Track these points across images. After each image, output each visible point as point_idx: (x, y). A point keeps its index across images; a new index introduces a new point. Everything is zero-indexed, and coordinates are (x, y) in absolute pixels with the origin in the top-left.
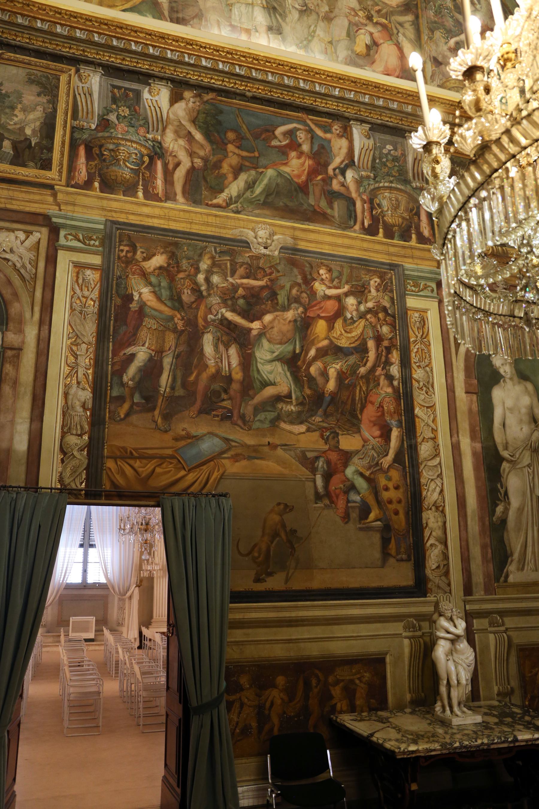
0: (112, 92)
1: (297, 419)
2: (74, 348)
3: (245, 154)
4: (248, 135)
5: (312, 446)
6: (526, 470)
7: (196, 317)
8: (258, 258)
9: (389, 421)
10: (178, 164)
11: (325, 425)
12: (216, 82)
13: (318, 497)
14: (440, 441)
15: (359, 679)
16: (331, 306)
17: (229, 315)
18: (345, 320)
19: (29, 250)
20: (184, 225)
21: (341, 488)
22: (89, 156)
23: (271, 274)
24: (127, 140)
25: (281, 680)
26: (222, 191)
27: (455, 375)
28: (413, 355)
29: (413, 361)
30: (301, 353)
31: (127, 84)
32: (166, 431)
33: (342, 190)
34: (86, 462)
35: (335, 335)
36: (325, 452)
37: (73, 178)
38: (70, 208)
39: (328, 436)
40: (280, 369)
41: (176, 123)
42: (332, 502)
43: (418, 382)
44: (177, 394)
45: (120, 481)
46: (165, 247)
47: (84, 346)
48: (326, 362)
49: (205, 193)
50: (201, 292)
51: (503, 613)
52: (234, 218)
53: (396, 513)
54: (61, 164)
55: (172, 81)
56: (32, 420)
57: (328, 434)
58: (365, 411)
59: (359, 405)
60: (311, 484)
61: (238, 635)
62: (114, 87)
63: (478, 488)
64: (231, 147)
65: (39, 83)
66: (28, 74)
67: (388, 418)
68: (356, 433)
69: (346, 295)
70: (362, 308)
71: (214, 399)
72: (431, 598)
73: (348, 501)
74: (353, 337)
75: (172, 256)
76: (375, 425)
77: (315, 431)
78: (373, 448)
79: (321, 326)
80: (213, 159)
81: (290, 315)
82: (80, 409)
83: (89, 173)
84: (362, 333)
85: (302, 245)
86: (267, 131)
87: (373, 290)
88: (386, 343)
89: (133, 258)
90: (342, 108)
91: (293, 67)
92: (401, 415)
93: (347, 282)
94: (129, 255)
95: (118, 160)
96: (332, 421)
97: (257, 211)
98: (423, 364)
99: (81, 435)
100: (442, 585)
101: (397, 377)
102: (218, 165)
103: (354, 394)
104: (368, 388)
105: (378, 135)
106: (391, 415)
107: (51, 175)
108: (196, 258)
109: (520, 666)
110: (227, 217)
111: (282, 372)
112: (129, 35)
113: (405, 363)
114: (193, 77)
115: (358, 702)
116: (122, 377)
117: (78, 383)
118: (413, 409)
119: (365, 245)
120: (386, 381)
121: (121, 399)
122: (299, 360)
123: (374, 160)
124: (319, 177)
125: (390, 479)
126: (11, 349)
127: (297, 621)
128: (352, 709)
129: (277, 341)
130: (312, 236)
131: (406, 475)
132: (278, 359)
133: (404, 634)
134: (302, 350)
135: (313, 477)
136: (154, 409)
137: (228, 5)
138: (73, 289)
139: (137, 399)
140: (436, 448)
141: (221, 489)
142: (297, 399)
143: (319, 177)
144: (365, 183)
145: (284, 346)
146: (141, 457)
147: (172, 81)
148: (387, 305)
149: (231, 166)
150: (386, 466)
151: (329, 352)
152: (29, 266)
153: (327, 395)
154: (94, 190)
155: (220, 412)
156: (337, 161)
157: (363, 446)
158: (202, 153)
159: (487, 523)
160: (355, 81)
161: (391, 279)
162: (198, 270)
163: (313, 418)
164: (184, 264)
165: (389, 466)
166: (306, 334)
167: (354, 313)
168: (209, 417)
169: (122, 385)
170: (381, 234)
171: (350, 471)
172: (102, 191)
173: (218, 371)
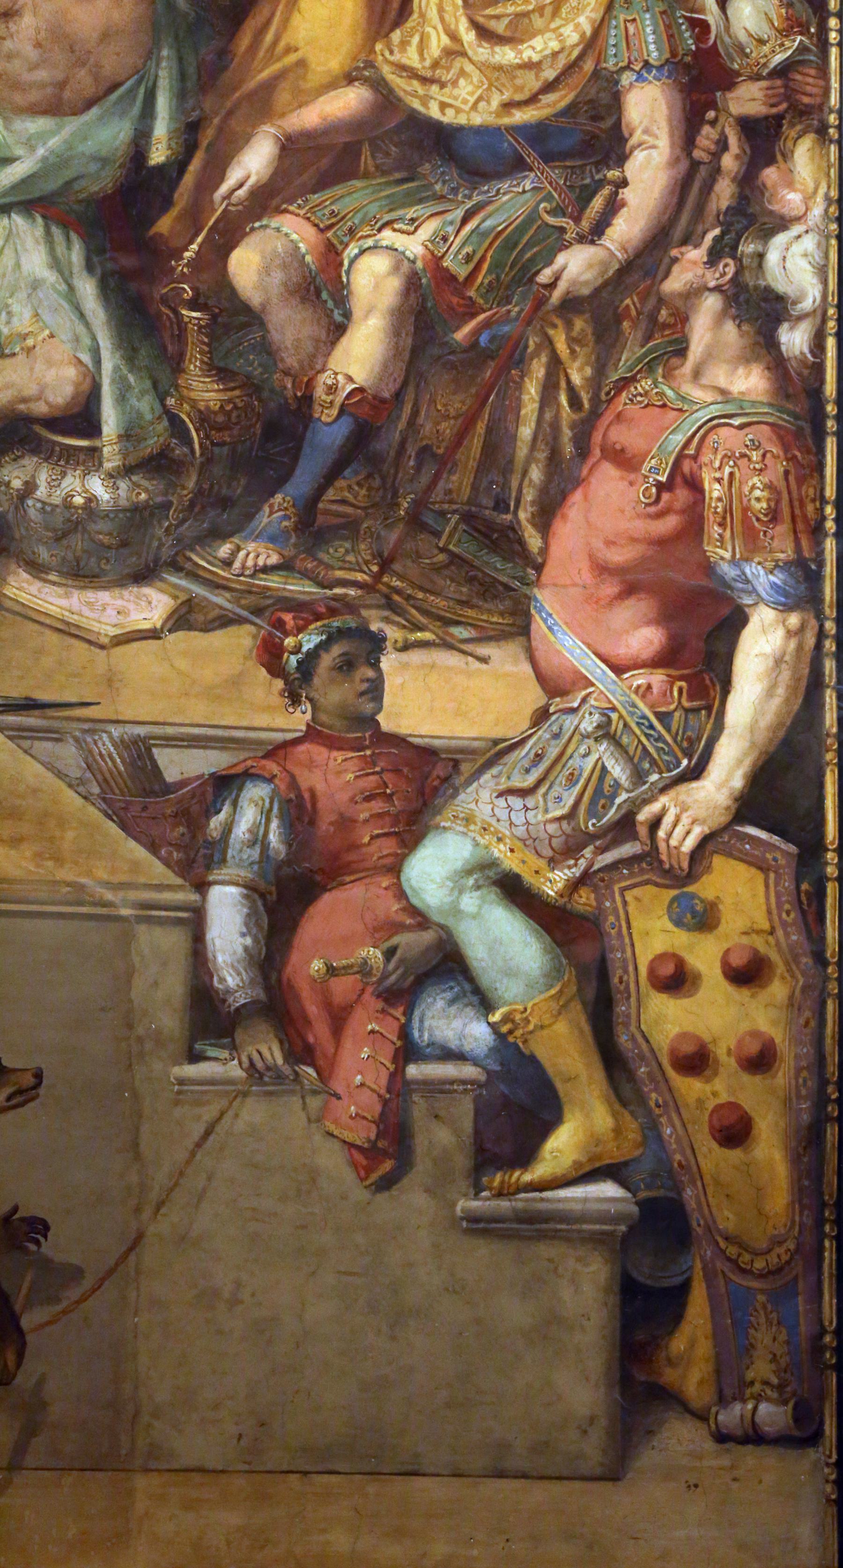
9: (728, 571)
21: (364, 969)
30: (180, 164)
35: (411, 58)
39: (313, 655)
48: (338, 219)
57: (310, 641)
59: (536, 474)
68: (499, 636)
74: (529, 66)
76: (629, 590)
77: (225, 621)
92: (817, 531)
101: (807, 304)
104: (600, 370)
111: (50, 277)
120: (730, 329)
122: (167, 203)
129: (34, 96)
131: (820, 894)
134: (190, 149)
135: (193, 897)
142: (128, 436)
145: (72, 125)
151: (366, 159)
153: (329, 415)
157: (541, 716)
163: (224, 550)
165: (705, 841)
166: (224, 54)
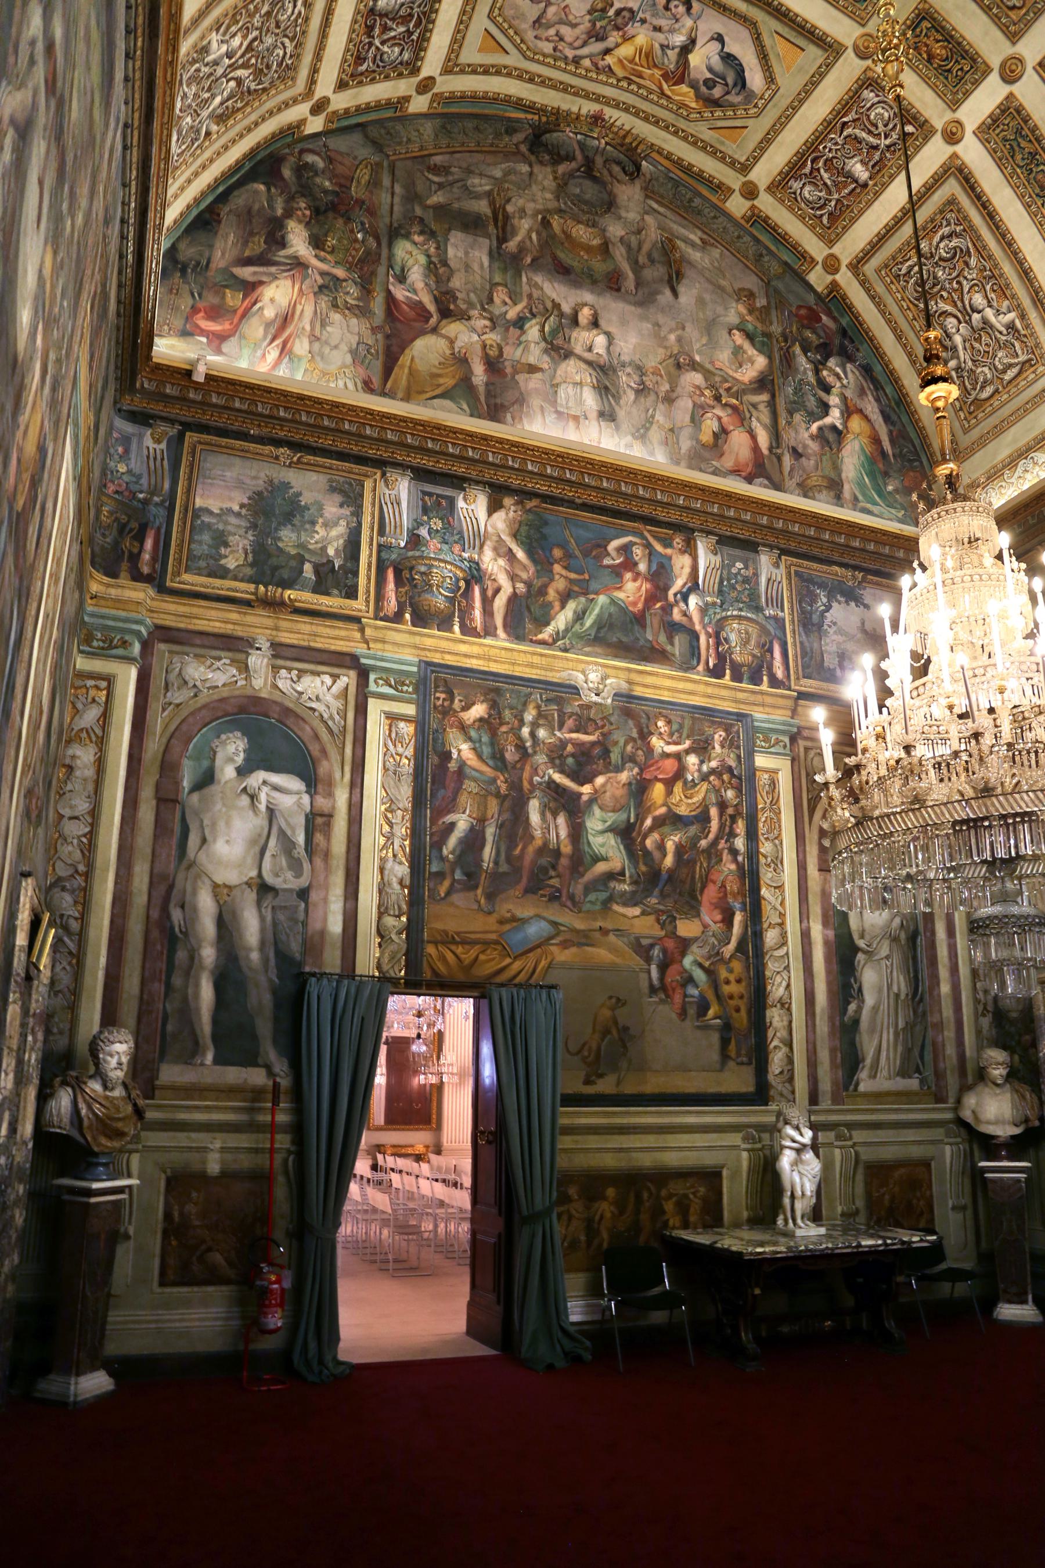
0: (423, 500)
1: (630, 900)
2: (389, 815)
3: (573, 576)
4: (577, 553)
5: (646, 932)
6: (883, 962)
7: (521, 779)
8: (588, 707)
10: (497, 590)
11: (661, 907)
12: (543, 488)
13: (653, 990)
14: (789, 928)
15: (694, 1193)
16: (670, 765)
17: (558, 777)
18: (685, 782)
19: (336, 697)
20: (506, 666)
22: (399, 582)
23: (603, 727)
24: (440, 560)
25: (611, 1192)
26: (548, 624)
27: (808, 849)
28: (761, 825)
29: (760, 832)
31: (439, 490)
32: (490, 913)
34: (405, 946)
36: (661, 939)
37: (382, 609)
38: (379, 646)
40: (613, 842)
41: (495, 538)
43: (766, 857)
44: (501, 870)
45: (442, 968)
46: (485, 695)
47: (399, 813)
49: (529, 626)
50: (525, 749)
51: (851, 1126)
52: (562, 658)
53: (738, 1010)
54: (368, 591)
55: (491, 485)
56: (346, 899)
58: (706, 891)
61: (565, 1142)
62: (425, 493)
63: (829, 983)
64: (557, 568)
65: (341, 491)
66: (330, 481)
69: (687, 752)
70: (705, 768)
71: (541, 877)
72: (773, 1107)
73: (685, 996)
75: (494, 705)
78: (714, 935)
79: (658, 790)
80: (538, 583)
81: (624, 776)
82: (396, 886)
83: (399, 602)
84: (704, 799)
85: (639, 691)
86: (599, 546)
87: (717, 747)
88: (730, 811)
89: (450, 708)
93: (688, 737)
94: (446, 704)
95: (431, 586)
96: (670, 903)
97: (587, 649)
98: (771, 836)
99: (399, 916)
100: (785, 1092)
102: (542, 591)
103: (694, 872)
105: (727, 550)
106: (734, 896)
107: (357, 605)
108: (520, 707)
109: (867, 1184)
110: (554, 657)
112: (447, 436)
113: (752, 835)
114: (515, 482)
115: (692, 1219)
116: (441, 850)
117: (395, 856)
118: (759, 889)
119: (710, 690)
121: (440, 875)
124: (658, 605)
125: (731, 971)
126: (322, 815)
127: (629, 1128)
128: (686, 1225)
130: (649, 680)
132: (611, 829)
133: (744, 1146)
136: (476, 887)
137: (553, 386)
138: (385, 745)
139: (458, 875)
140: (784, 935)
141: (549, 981)
142: (631, 877)
143: (658, 605)
144: (711, 611)
146: (464, 942)
147: (491, 485)
148: (733, 763)
149: (558, 592)
152: (337, 717)
154: (405, 623)
155: (547, 891)
156: (679, 584)
158: (524, 576)
159: (837, 1023)
160: (703, 489)
161: (738, 732)
162: (522, 722)
164: (507, 714)
167: (696, 775)
168: (535, 897)
169: (442, 859)
170: (728, 677)
171: (687, 961)
172: (414, 625)
173: (546, 844)
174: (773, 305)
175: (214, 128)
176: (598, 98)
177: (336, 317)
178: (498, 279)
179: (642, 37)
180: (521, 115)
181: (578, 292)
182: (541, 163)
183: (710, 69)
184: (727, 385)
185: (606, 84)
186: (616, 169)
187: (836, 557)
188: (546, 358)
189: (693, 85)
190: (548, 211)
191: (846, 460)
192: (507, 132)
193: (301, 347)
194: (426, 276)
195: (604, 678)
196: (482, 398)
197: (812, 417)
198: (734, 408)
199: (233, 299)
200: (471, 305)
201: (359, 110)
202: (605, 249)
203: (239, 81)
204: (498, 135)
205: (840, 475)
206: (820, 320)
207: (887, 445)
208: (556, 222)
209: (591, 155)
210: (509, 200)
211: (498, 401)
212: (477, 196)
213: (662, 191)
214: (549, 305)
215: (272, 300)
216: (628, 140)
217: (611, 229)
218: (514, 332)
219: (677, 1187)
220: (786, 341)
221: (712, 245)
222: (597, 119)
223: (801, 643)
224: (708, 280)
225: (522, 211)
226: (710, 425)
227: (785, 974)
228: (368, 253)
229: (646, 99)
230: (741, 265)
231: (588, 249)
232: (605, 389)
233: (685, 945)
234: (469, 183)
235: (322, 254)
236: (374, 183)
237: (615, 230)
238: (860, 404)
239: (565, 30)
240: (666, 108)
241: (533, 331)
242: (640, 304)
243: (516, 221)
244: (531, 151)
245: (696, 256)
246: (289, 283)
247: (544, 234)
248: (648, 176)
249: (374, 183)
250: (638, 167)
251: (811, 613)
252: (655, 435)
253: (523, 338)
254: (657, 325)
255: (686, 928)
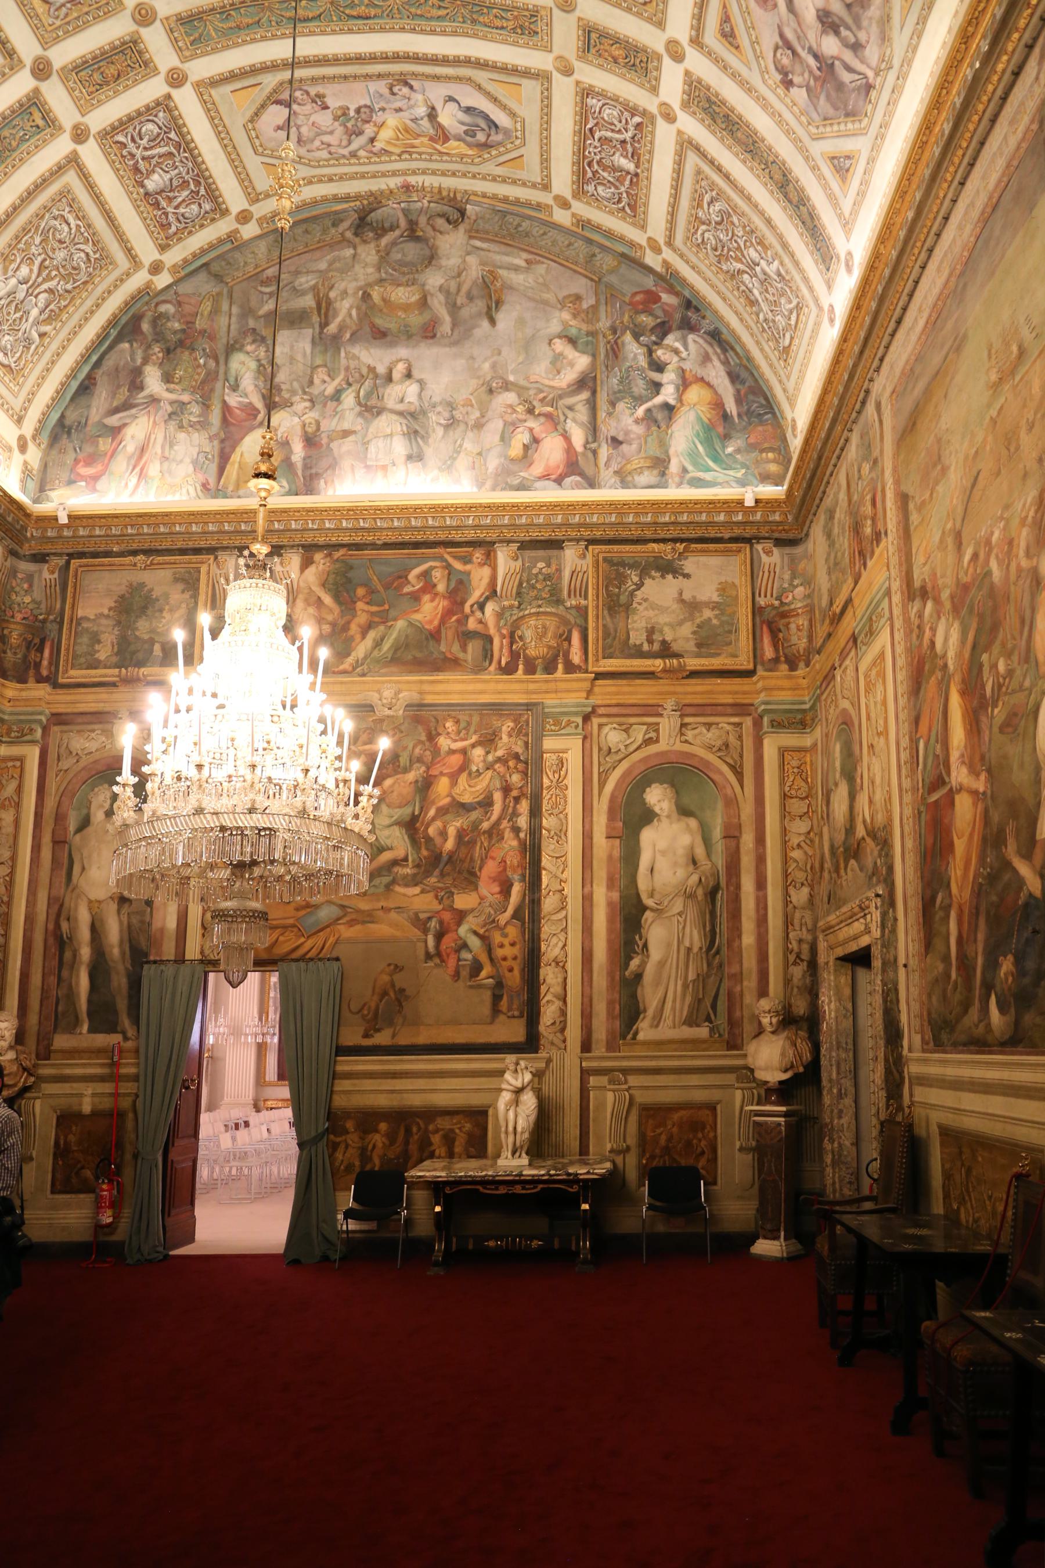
1: (413, 881)
3: (374, 609)
4: (380, 587)
5: (425, 907)
13: (428, 956)
16: (456, 760)
18: (470, 774)
26: (349, 655)
27: (595, 819)
28: (545, 802)
33: (479, 628)
36: (438, 912)
40: (398, 833)
42: (442, 961)
43: (549, 831)
51: (626, 1071)
53: (511, 970)
55: (303, 546)
60: (422, 945)
63: (610, 942)
64: (360, 605)
67: (509, 874)
69: (473, 746)
70: (490, 758)
72: (543, 1054)
73: (459, 960)
79: (443, 785)
80: (341, 622)
81: (411, 776)
85: (429, 699)
86: (400, 577)
90: (482, 535)
91: (417, 509)
93: (475, 732)
96: (449, 881)
97: (383, 671)
98: (556, 811)
110: (353, 682)
114: (321, 540)
115: (458, 1149)
118: (539, 861)
119: (500, 687)
123: (520, 584)
124: (454, 618)
125: (506, 936)
132: (398, 823)
144: (507, 614)
148: (519, 749)
149: (359, 626)
150: (502, 922)
156: (476, 596)
158: (330, 618)
159: (617, 978)
167: (481, 765)
171: (463, 930)
174: (603, 301)
175: (46, 328)
176: (394, 174)
177: (182, 436)
178: (318, 361)
179: (392, 121)
180: (345, 206)
181: (394, 351)
182: (365, 242)
183: (463, 123)
184: (541, 396)
185: (391, 161)
186: (440, 222)
187: (648, 534)
188: (360, 420)
189: (458, 138)
190: (370, 285)
191: (676, 434)
192: (334, 225)
193: (154, 469)
194: (256, 379)
195: (398, 693)
196: (300, 473)
197: (639, 400)
198: (548, 416)
199: (104, 444)
200: (294, 393)
201: (195, 256)
202: (424, 303)
203: (50, 291)
204: (325, 231)
205: (667, 452)
206: (660, 298)
207: (731, 407)
208: (376, 294)
209: (414, 218)
210: (331, 288)
211: (313, 471)
212: (303, 293)
213: (487, 226)
214: (365, 371)
215: (133, 437)
216: (445, 193)
217: (431, 281)
218: (331, 405)
219: (444, 1123)
220: (614, 332)
221: (539, 262)
222: (407, 188)
223: (604, 626)
224: (530, 299)
225: (344, 293)
226: (522, 437)
227: (562, 936)
228: (208, 374)
229: (431, 160)
230: (569, 273)
231: (406, 308)
232: (413, 434)
233: (461, 916)
234: (296, 283)
235: (172, 386)
236: (215, 311)
237: (434, 280)
238: (700, 372)
239: (326, 138)
240: (452, 162)
241: (349, 399)
242: (456, 343)
243: (337, 305)
244: (356, 234)
245: (518, 279)
246: (145, 419)
247: (364, 308)
248: (473, 217)
249: (215, 311)
250: (462, 213)
251: (618, 595)
252: (463, 462)
253: (339, 409)
254: (472, 358)
255: (463, 901)
